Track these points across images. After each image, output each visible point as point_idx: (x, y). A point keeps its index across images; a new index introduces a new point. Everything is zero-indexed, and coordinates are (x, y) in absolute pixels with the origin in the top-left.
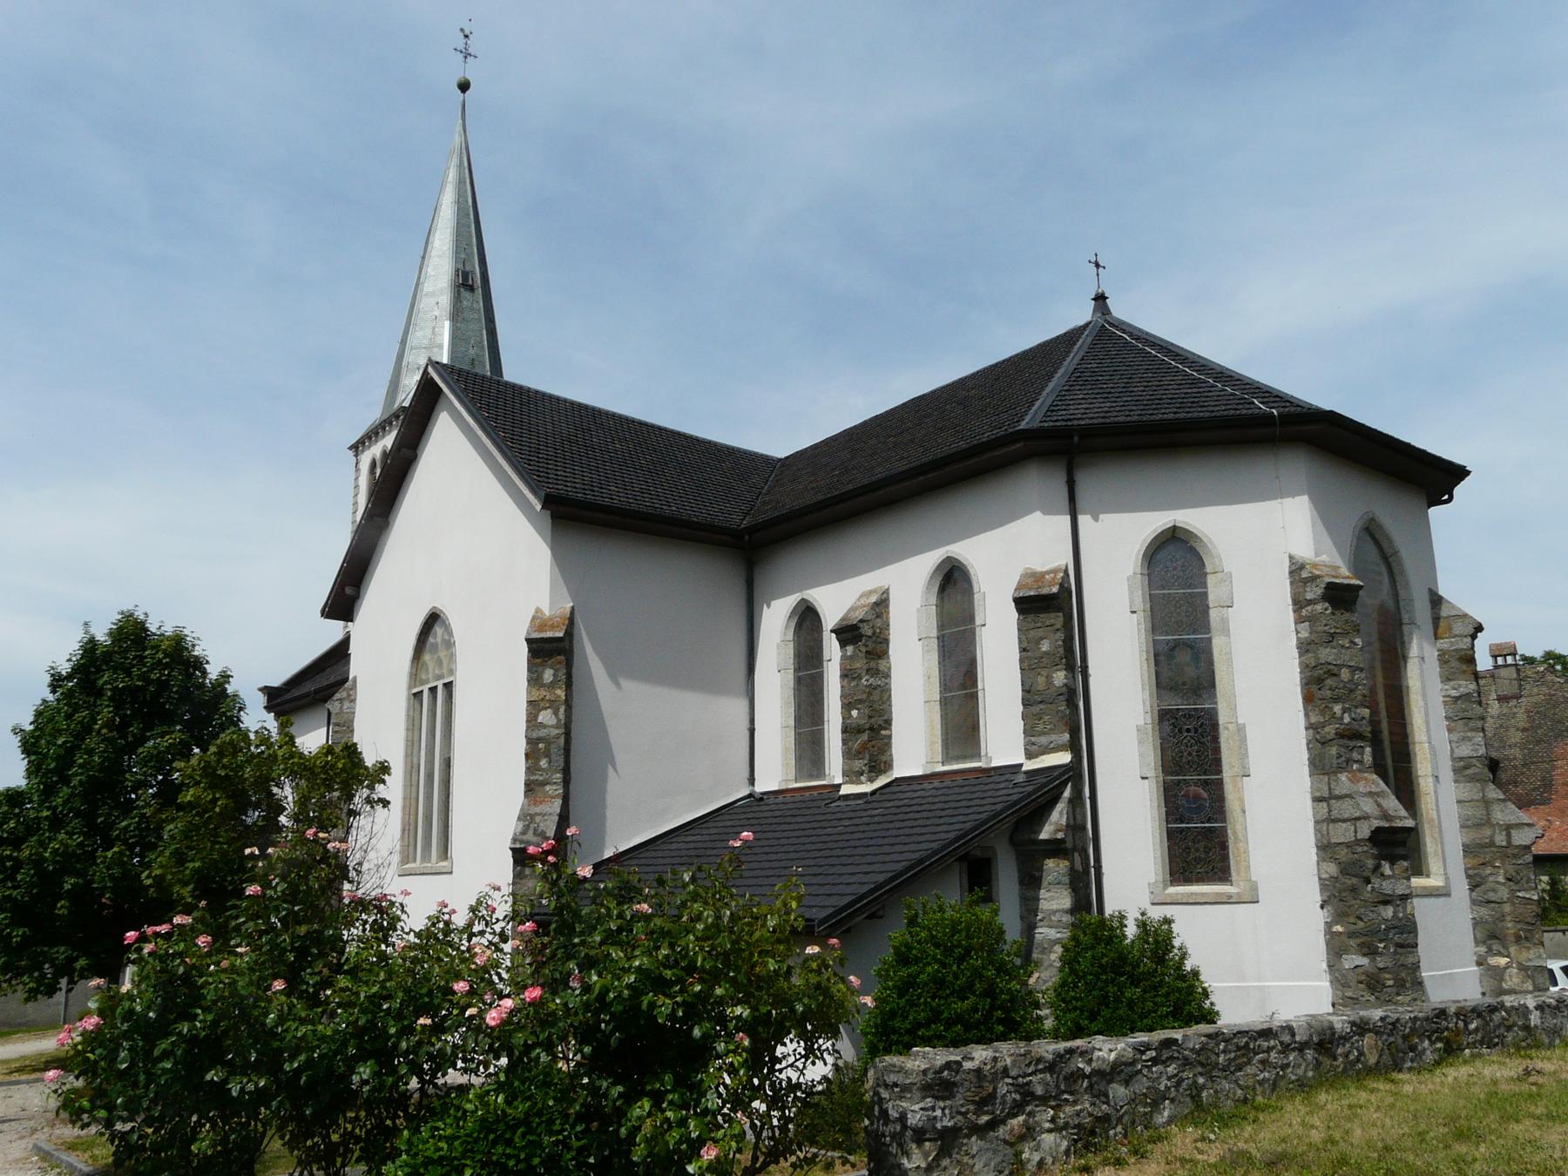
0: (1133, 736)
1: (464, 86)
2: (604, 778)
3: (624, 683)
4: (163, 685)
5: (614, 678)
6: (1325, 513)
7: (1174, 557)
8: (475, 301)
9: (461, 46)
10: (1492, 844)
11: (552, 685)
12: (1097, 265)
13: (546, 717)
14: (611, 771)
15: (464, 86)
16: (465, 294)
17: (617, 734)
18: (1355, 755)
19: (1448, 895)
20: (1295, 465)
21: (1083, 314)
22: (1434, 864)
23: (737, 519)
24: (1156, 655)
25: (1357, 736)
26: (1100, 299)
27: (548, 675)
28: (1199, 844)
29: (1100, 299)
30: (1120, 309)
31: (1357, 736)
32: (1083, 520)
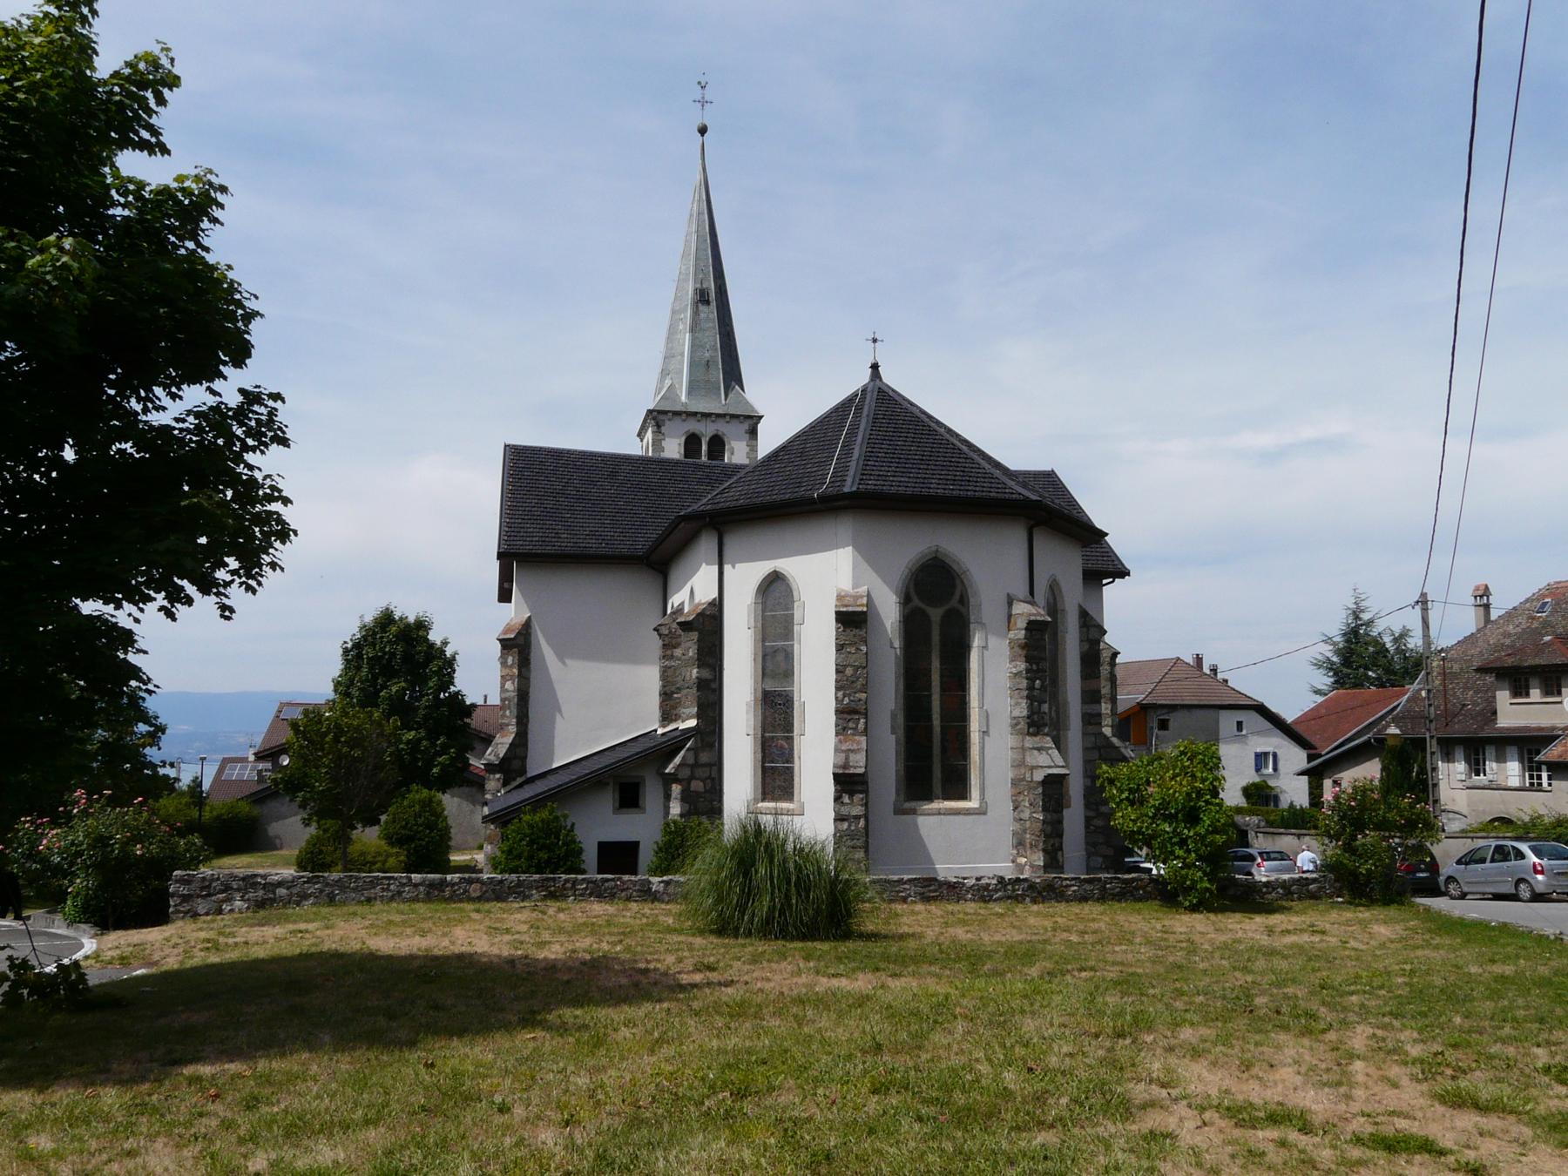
0: (744, 708)
1: (703, 131)
2: (553, 722)
3: (568, 661)
4: (393, 655)
5: (561, 657)
6: (867, 554)
7: (774, 589)
8: (710, 313)
9: (699, 97)
10: (1023, 779)
11: (511, 667)
12: (875, 341)
13: (509, 685)
14: (558, 717)
15: (703, 131)
16: (701, 307)
17: (562, 693)
18: (851, 725)
19: (985, 813)
20: (845, 526)
21: (859, 379)
22: (975, 792)
23: (641, 545)
24: (764, 657)
25: (855, 712)
26: (875, 367)
27: (510, 660)
28: (776, 776)
29: (875, 367)
30: (889, 378)
31: (855, 712)
32: (727, 568)
